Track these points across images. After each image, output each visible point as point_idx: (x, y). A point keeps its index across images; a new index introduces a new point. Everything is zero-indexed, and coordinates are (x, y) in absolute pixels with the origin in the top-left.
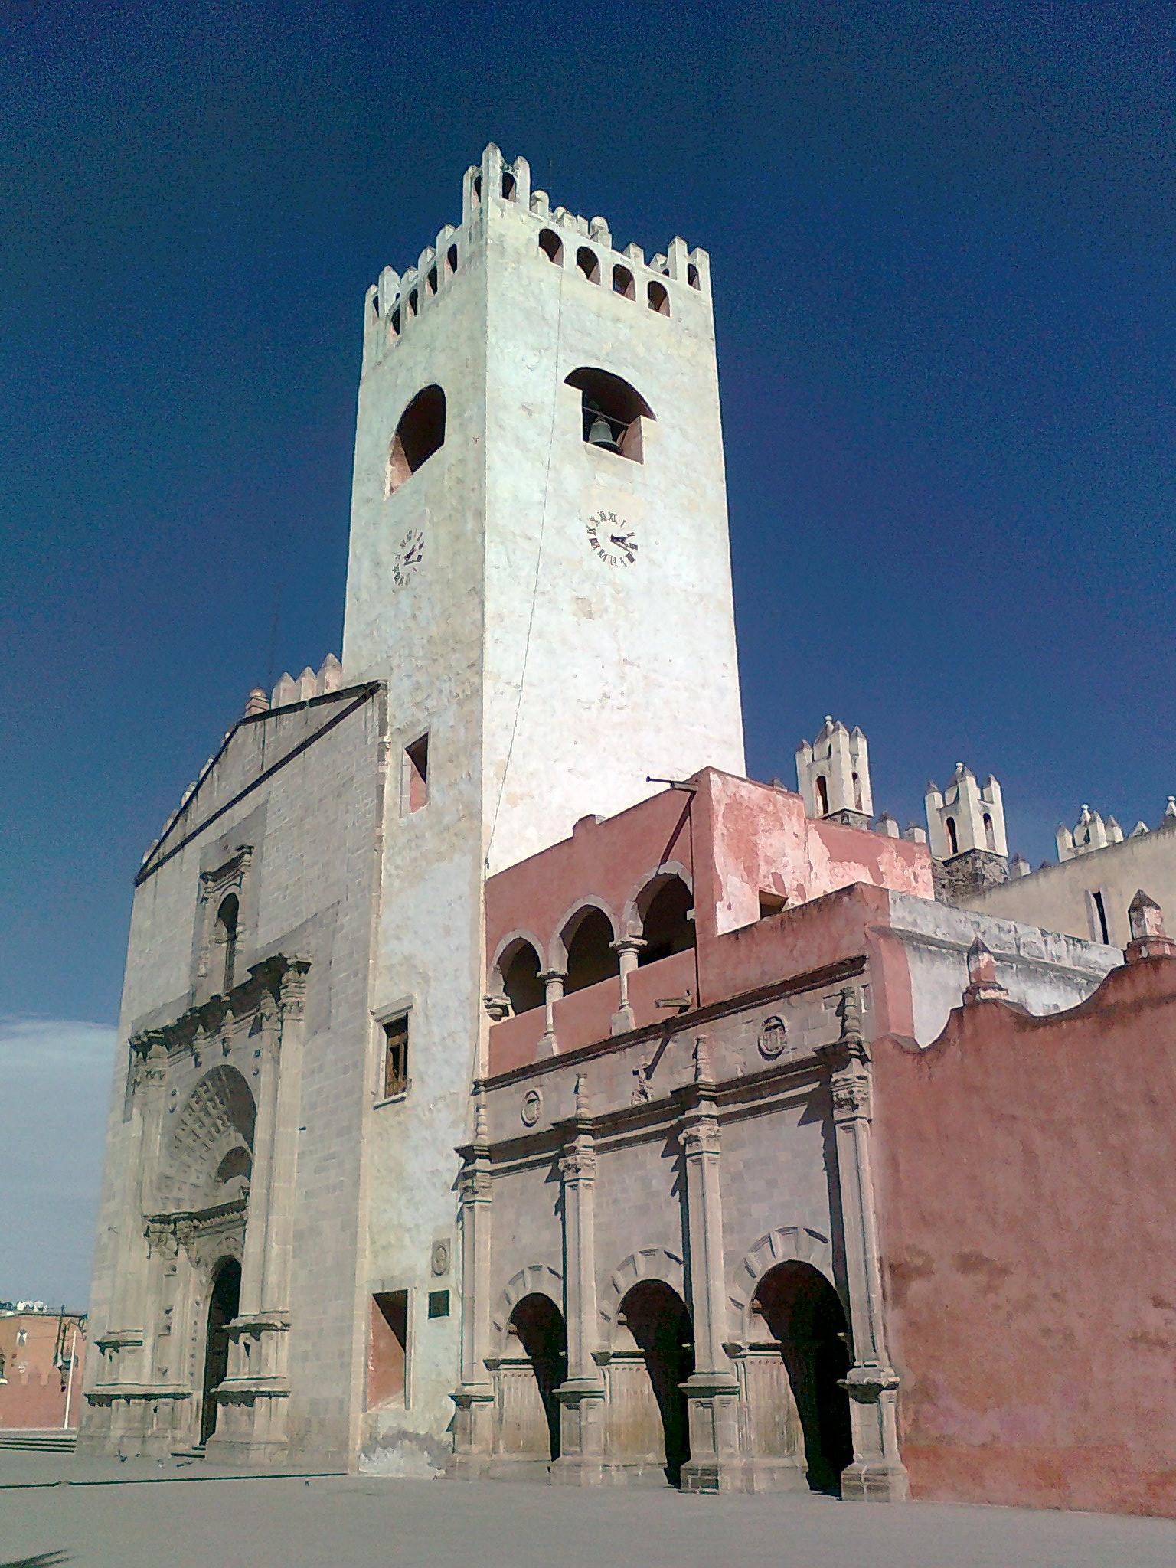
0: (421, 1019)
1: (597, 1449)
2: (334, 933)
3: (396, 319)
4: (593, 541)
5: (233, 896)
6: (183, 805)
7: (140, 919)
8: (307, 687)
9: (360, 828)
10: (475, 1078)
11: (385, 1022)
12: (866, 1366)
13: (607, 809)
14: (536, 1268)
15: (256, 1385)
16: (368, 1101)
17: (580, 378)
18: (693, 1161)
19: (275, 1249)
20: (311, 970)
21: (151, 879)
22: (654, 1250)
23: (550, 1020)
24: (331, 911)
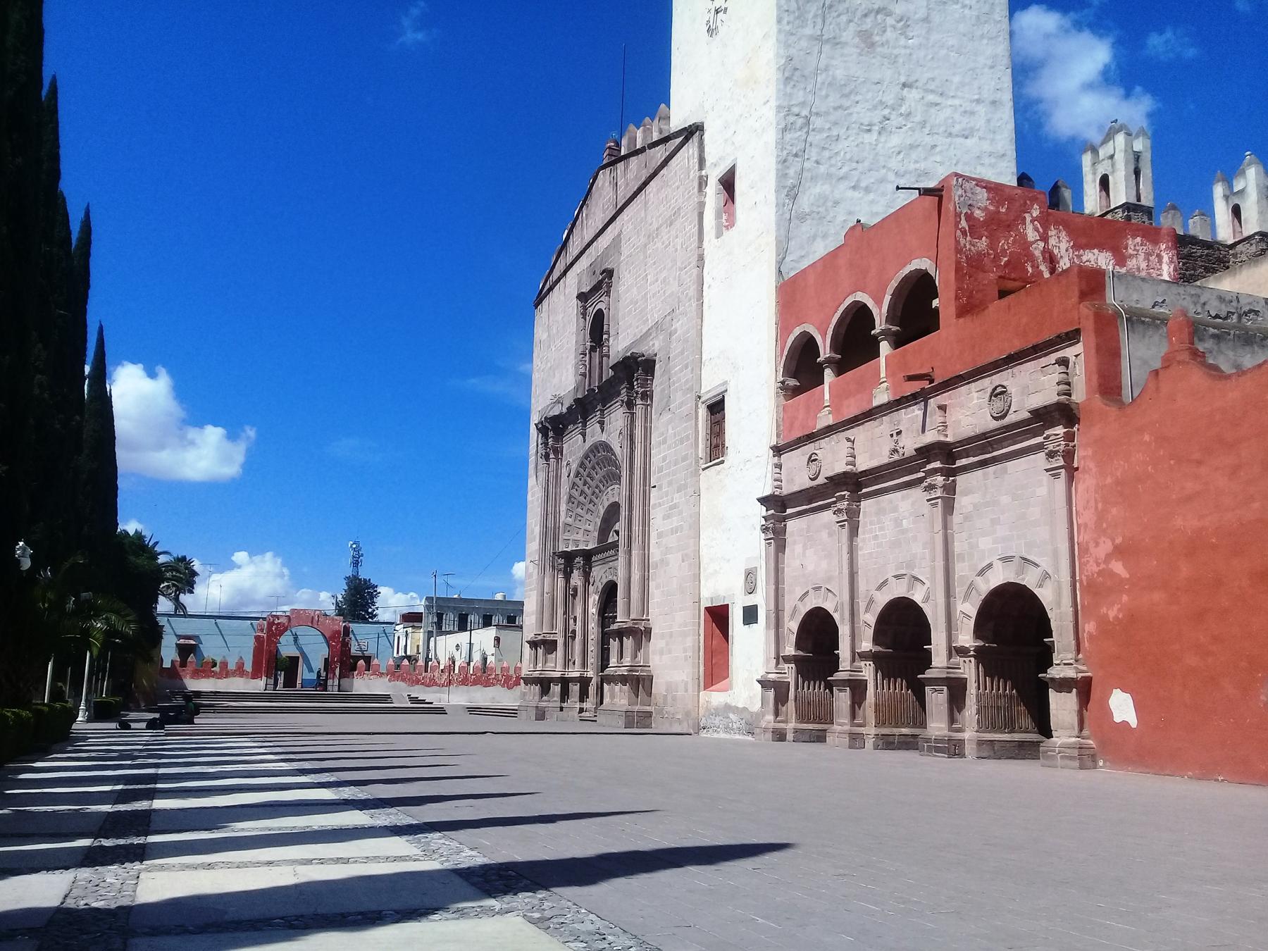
2: (671, 335)
7: (540, 333)
11: (709, 403)
14: (817, 589)
23: (827, 396)
24: (668, 318)
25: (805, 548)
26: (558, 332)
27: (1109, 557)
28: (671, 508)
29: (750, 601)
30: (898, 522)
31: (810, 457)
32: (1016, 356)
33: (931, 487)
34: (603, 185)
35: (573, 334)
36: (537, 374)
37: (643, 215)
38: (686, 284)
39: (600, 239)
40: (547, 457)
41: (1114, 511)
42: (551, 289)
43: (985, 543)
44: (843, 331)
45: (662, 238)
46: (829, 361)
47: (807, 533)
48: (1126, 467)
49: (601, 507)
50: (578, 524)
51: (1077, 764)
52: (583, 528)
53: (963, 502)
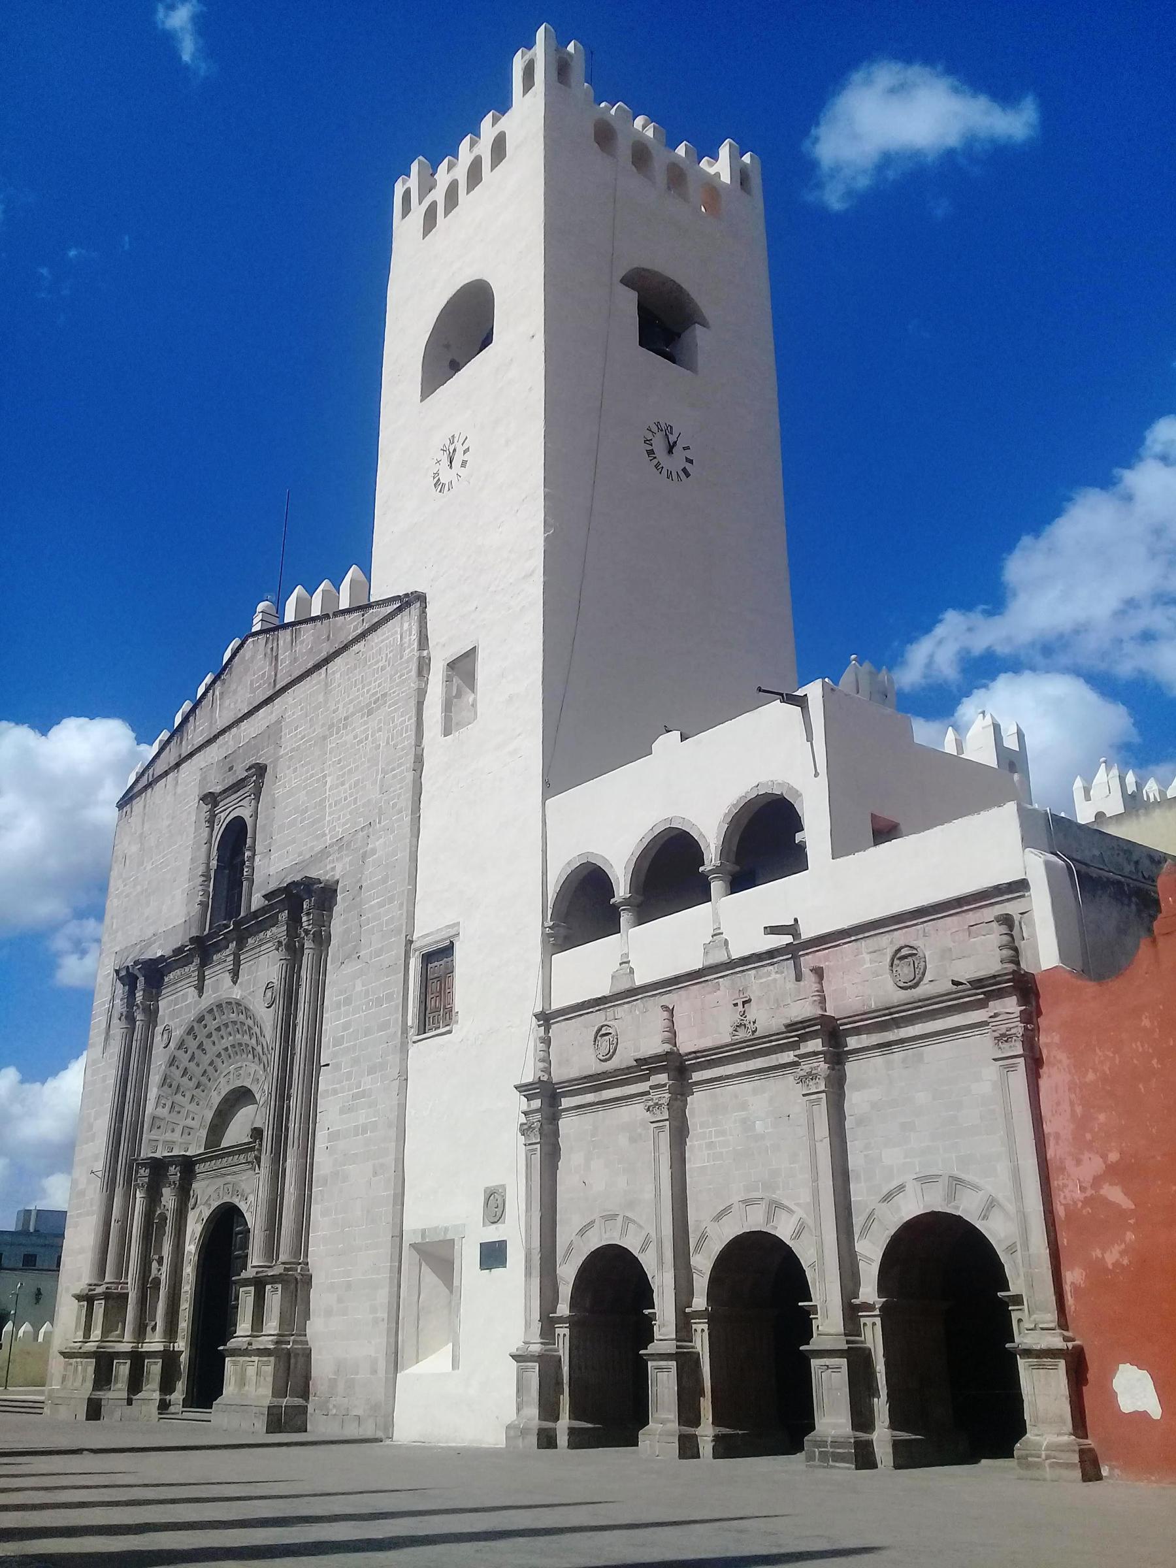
2: (364, 857)
4: (650, 452)
6: (176, 725)
9: (395, 746)
17: (637, 280)
21: (138, 804)
27: (1097, 1181)
28: (355, 1097)
29: (492, 1234)
30: (747, 1125)
31: (600, 1030)
32: (930, 910)
33: (812, 1076)
34: (253, 657)
36: (115, 900)
37: (321, 699)
38: (394, 791)
40: (130, 1018)
41: (1102, 1117)
42: (150, 785)
43: (892, 1157)
44: (646, 865)
45: (354, 729)
46: (626, 902)
48: (1117, 1061)
49: (214, 1094)
50: (173, 1117)
51: (1078, 1474)
52: (183, 1123)
53: (855, 1101)
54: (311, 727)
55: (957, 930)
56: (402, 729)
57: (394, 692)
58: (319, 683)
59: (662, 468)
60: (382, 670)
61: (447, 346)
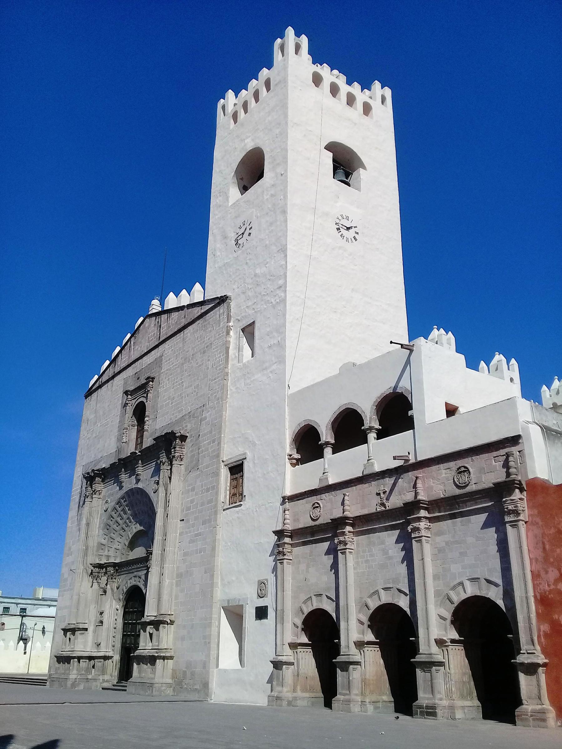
0: (251, 465)
1: (358, 692)
2: (201, 421)
3: (235, 116)
4: (338, 229)
5: (142, 402)
8: (185, 298)
10: (283, 495)
11: (230, 466)
12: (528, 653)
13: (360, 360)
15: (157, 653)
16: (220, 507)
18: (416, 541)
19: (167, 582)
20: (188, 440)
21: (94, 395)
22: (390, 588)
24: (199, 410)
25: (308, 566)
26: (104, 414)
28: (196, 535)
29: (261, 603)
35: (117, 416)
38: (216, 389)
39: (145, 358)
42: (100, 387)
47: (310, 556)
52: (115, 546)
54: (176, 359)
55: (487, 459)
56: (219, 360)
57: (215, 343)
58: (180, 338)
59: (344, 236)
60: (210, 332)
61: (242, 179)
